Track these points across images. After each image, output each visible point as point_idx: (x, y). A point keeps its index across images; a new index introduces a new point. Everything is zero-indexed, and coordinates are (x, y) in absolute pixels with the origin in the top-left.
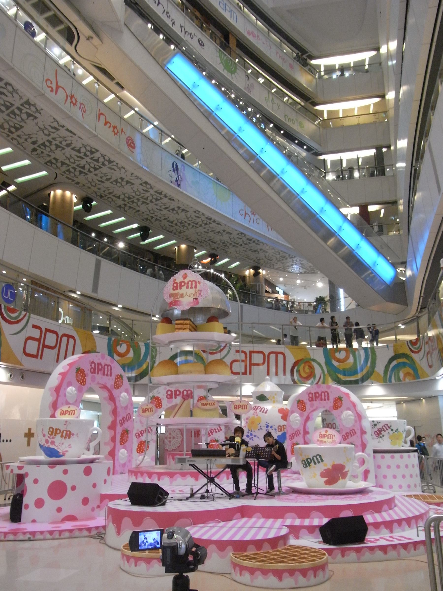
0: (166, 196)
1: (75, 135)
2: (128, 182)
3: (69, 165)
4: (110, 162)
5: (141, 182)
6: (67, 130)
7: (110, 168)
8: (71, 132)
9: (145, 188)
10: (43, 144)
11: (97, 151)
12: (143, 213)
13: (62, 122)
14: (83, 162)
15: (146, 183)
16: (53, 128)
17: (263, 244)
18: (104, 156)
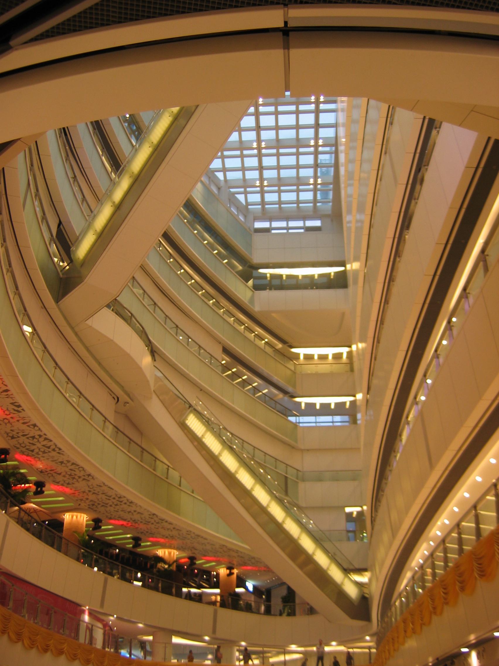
0: (166, 522)
1: (113, 489)
2: (139, 513)
3: (95, 502)
4: (131, 502)
5: (149, 513)
6: (109, 487)
7: (129, 506)
8: (111, 488)
9: (151, 517)
10: (84, 492)
11: (125, 497)
12: (141, 529)
13: (107, 483)
14: (108, 501)
15: (154, 514)
16: (97, 485)
17: (241, 552)
18: (128, 500)
